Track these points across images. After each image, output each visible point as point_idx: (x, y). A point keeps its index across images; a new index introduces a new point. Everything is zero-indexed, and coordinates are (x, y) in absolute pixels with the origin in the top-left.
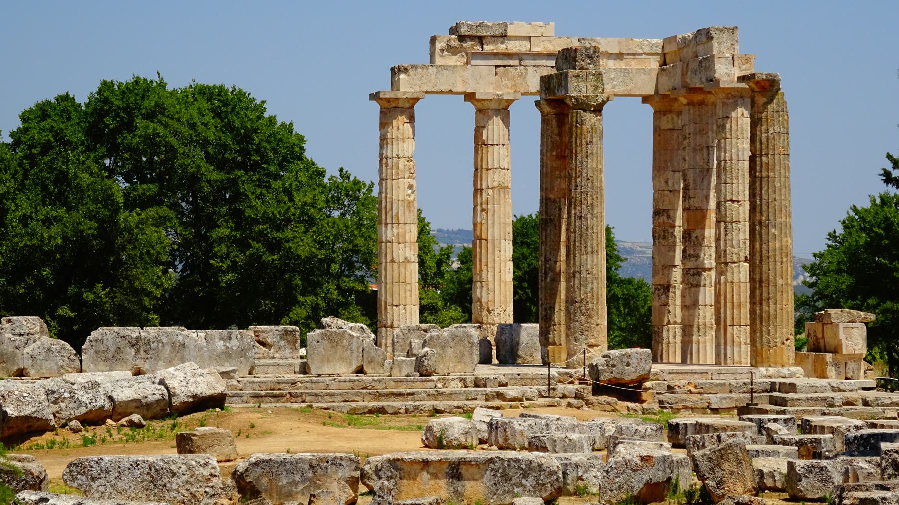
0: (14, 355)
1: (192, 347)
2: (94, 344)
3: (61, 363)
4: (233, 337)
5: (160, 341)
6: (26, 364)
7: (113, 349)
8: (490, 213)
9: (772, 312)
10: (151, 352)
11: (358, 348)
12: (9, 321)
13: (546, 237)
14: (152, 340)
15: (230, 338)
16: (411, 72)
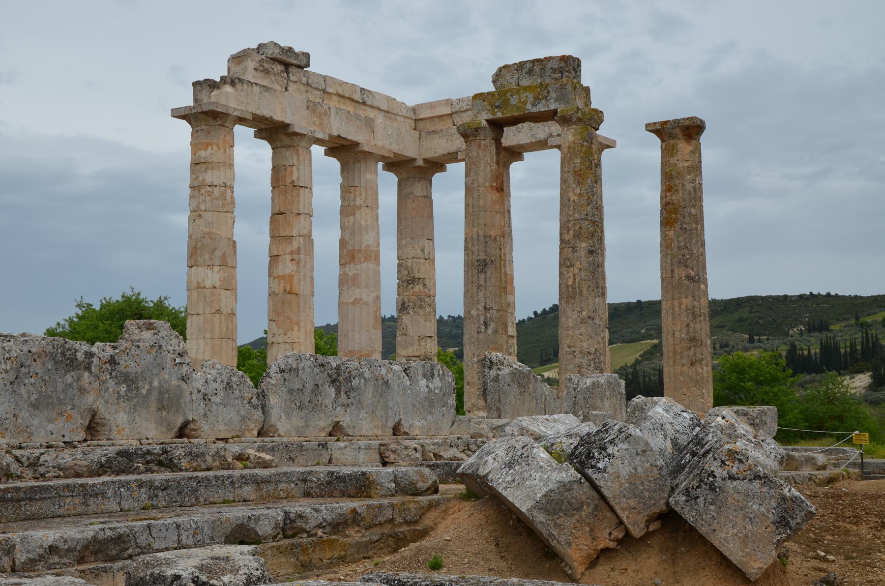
0: (179, 395)
1: (396, 388)
2: (286, 375)
3: (242, 413)
4: (436, 375)
5: (361, 375)
6: (193, 411)
7: (309, 387)
8: (302, 264)
9: (705, 374)
10: (352, 395)
11: (541, 396)
12: (149, 327)
13: (485, 282)
14: (353, 373)
15: (433, 376)
16: (239, 86)
